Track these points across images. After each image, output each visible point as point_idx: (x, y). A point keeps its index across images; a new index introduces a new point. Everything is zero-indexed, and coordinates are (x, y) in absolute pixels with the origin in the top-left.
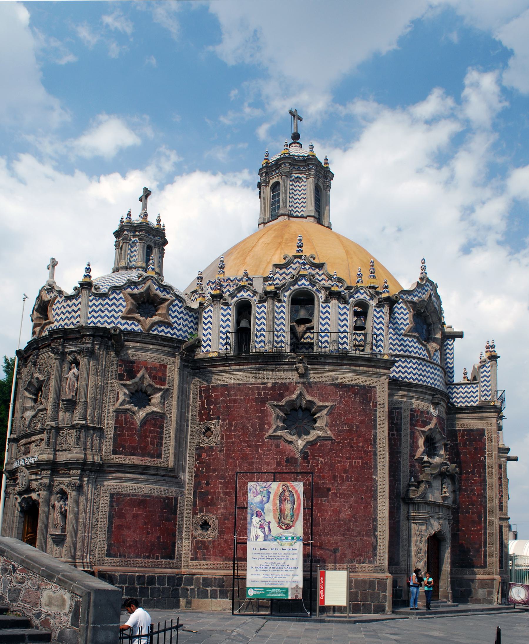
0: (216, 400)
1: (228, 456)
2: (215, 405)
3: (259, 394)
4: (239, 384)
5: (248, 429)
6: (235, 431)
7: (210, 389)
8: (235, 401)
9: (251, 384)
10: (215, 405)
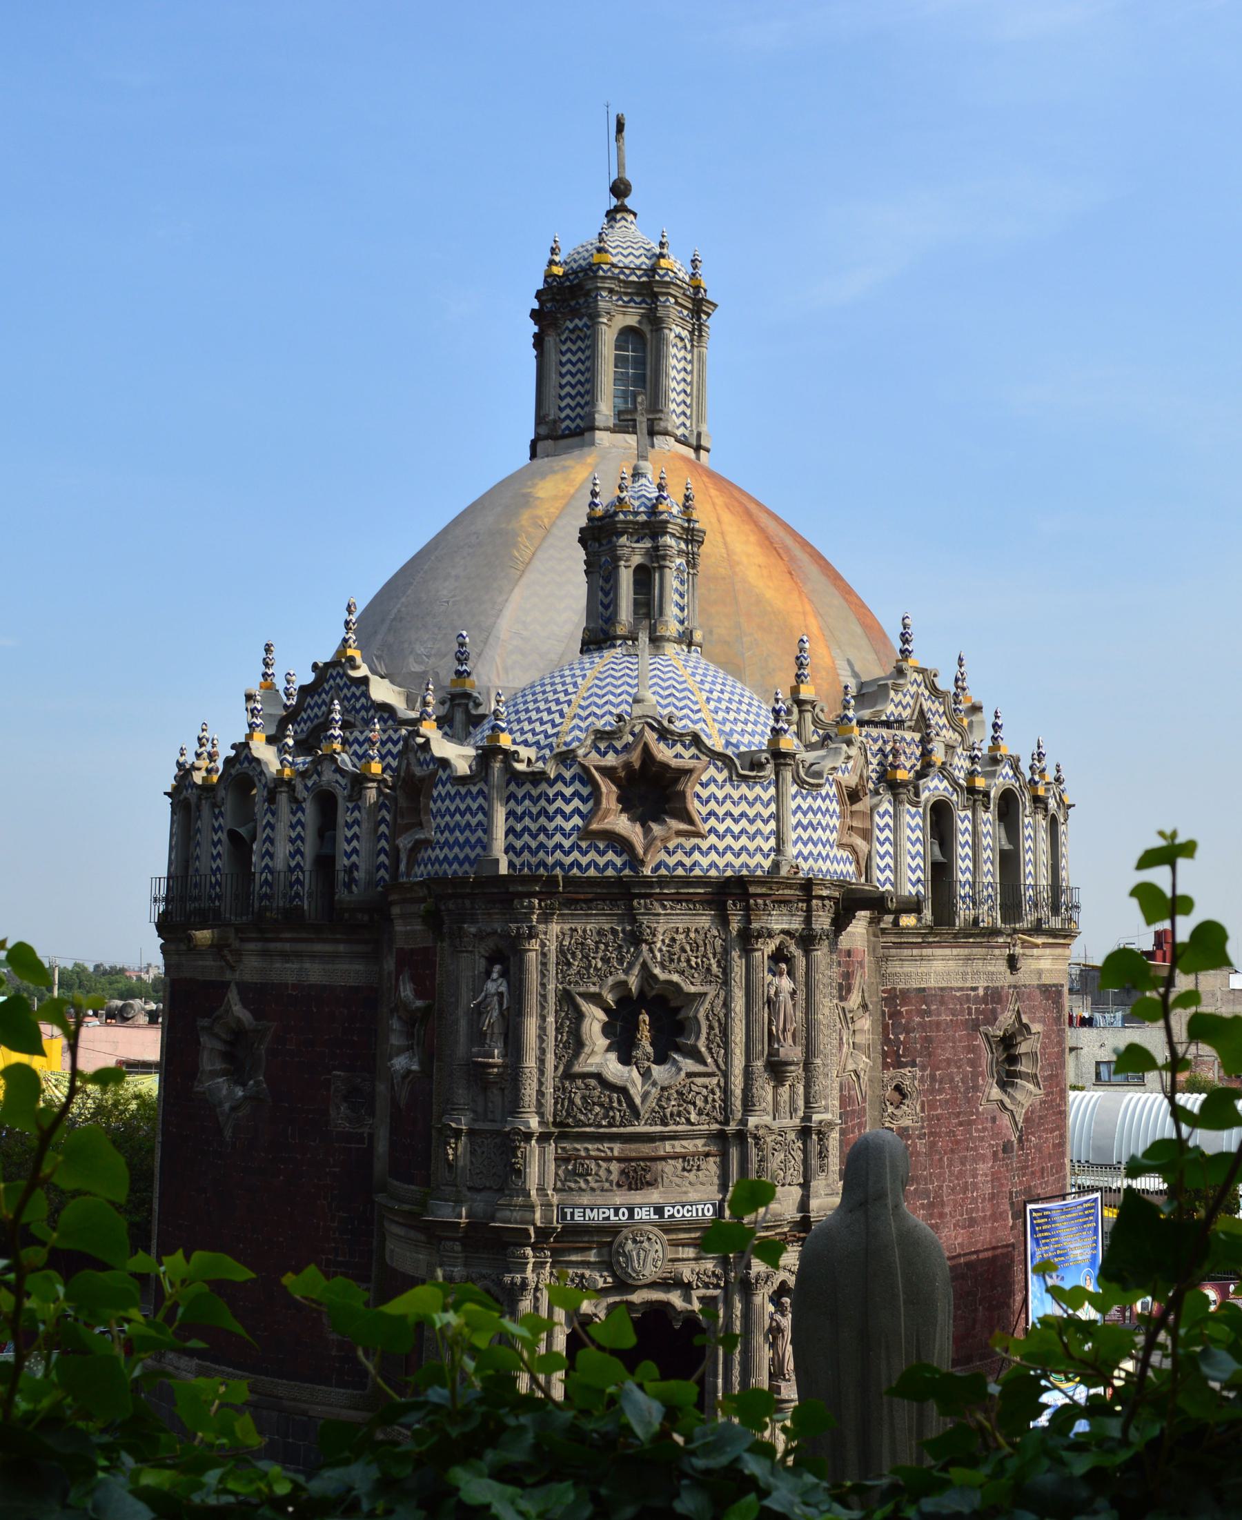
0: (908, 1022)
1: (933, 1145)
2: (908, 1033)
3: (970, 1014)
4: (942, 989)
5: (957, 1086)
6: (940, 1091)
7: (896, 997)
8: (938, 1024)
9: (961, 989)
10: (908, 1033)
